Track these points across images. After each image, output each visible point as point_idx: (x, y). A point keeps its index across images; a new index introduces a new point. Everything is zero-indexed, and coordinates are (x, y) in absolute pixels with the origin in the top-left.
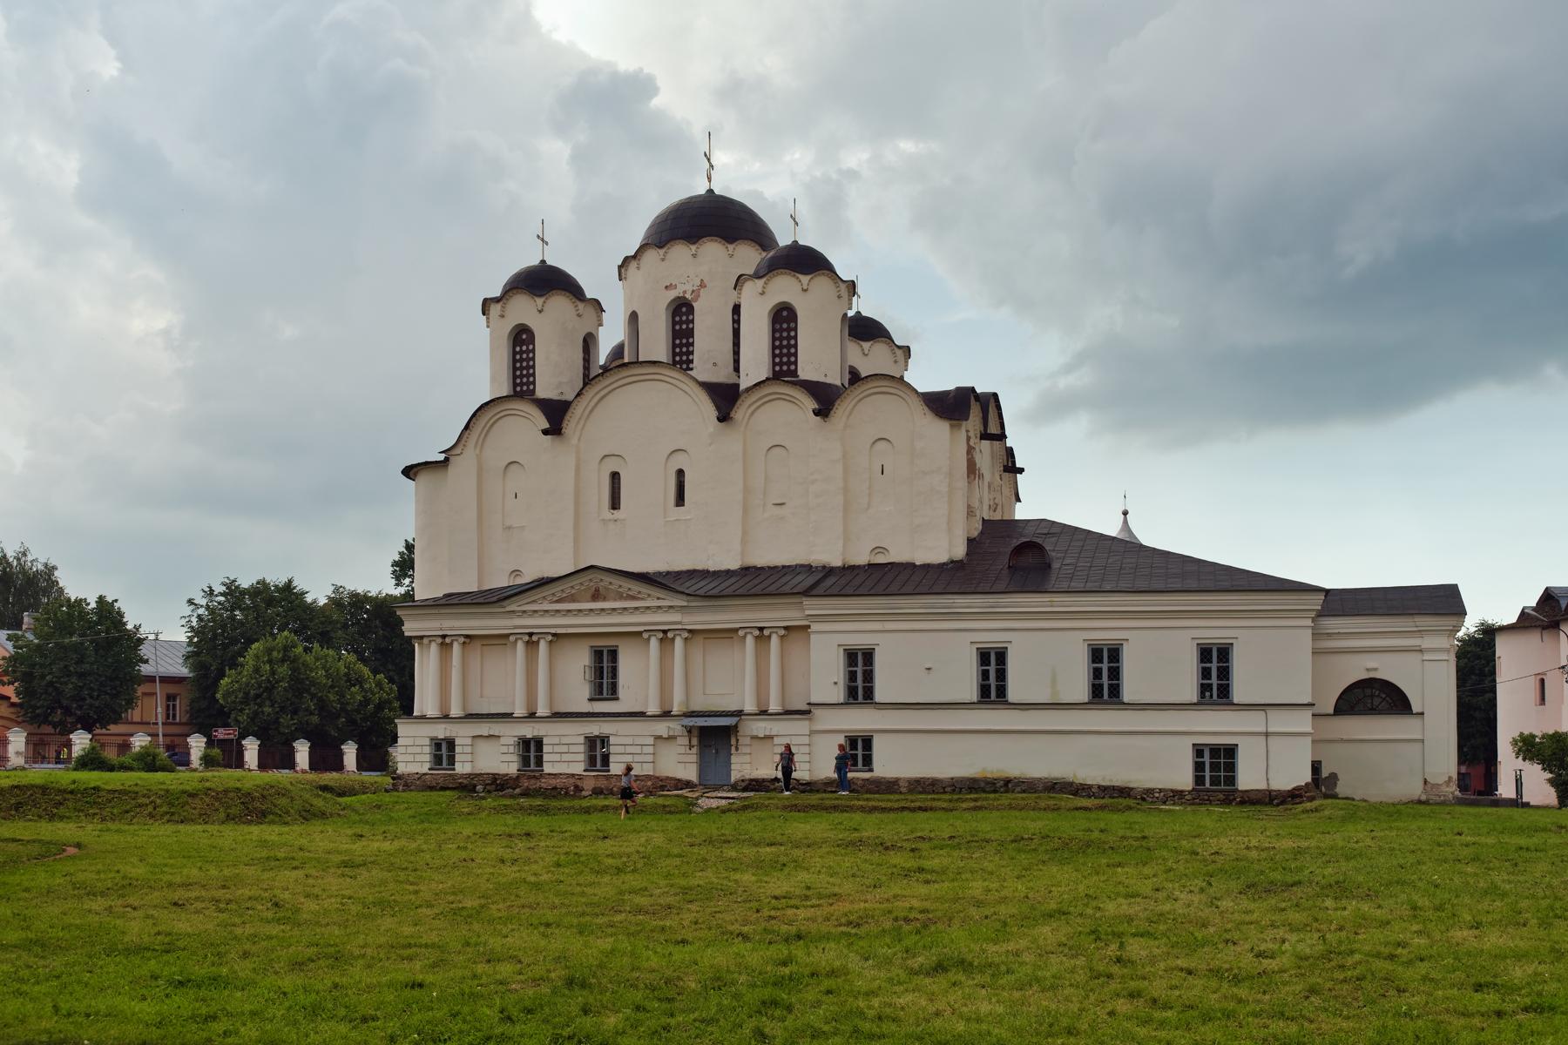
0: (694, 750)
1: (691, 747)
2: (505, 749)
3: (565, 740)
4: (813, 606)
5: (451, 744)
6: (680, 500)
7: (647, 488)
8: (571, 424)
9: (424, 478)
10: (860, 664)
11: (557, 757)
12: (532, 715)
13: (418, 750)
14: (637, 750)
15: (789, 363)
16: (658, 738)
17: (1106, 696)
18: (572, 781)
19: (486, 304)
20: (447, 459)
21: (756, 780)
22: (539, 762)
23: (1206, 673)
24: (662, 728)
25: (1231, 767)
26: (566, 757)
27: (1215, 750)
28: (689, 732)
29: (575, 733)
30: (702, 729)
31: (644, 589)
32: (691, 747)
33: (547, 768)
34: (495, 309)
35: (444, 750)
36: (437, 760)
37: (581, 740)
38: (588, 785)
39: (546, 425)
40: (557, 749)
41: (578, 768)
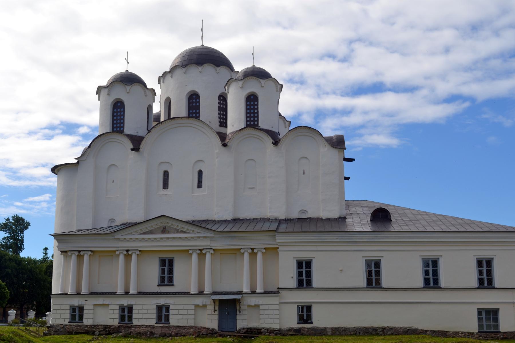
0: (217, 313)
1: (215, 311)
2: (112, 312)
3: (145, 307)
4: (280, 238)
5: (81, 309)
6: (200, 186)
7: (182, 179)
8: (143, 146)
9: (62, 173)
11: (141, 316)
12: (127, 293)
13: (63, 312)
14: (185, 312)
15: (254, 121)
16: (197, 306)
17: (432, 284)
18: (149, 329)
19: (100, 90)
20: (78, 162)
21: (251, 329)
22: (130, 318)
23: (480, 273)
24: (199, 301)
25: (496, 320)
26: (145, 316)
27: (488, 312)
28: (214, 303)
29: (152, 303)
30: (220, 301)
31: (191, 228)
32: (215, 311)
33: (135, 322)
34: (104, 92)
35: (77, 313)
36: (73, 317)
37: (155, 307)
38: (158, 331)
39: (132, 147)
40: (141, 311)
41: (153, 322)
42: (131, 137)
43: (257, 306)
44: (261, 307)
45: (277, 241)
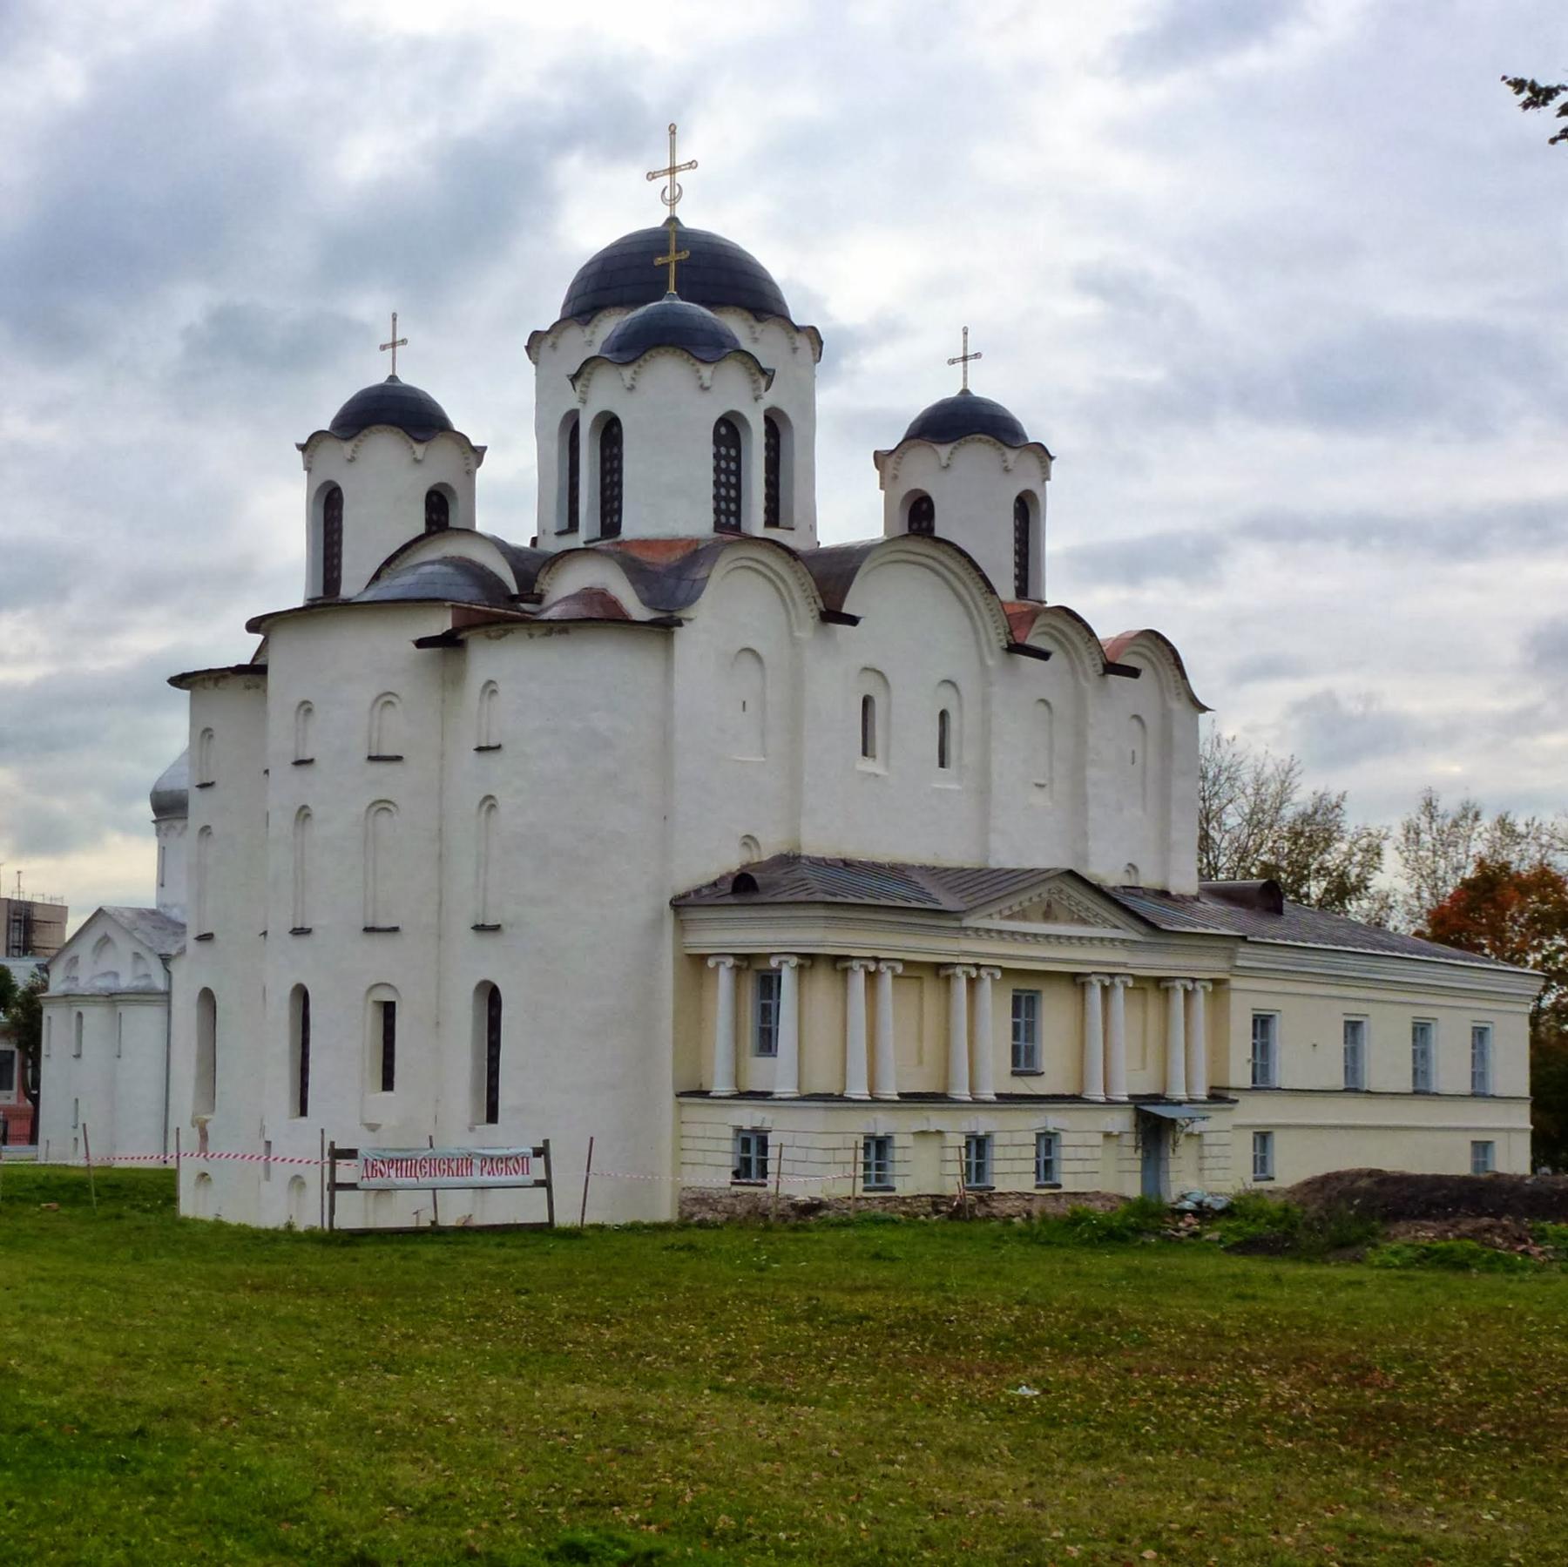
0: (1139, 1154)
1: (1137, 1148)
16: (1107, 1135)
43: (1200, 1135)
44: (1208, 1139)
45: (1239, 963)
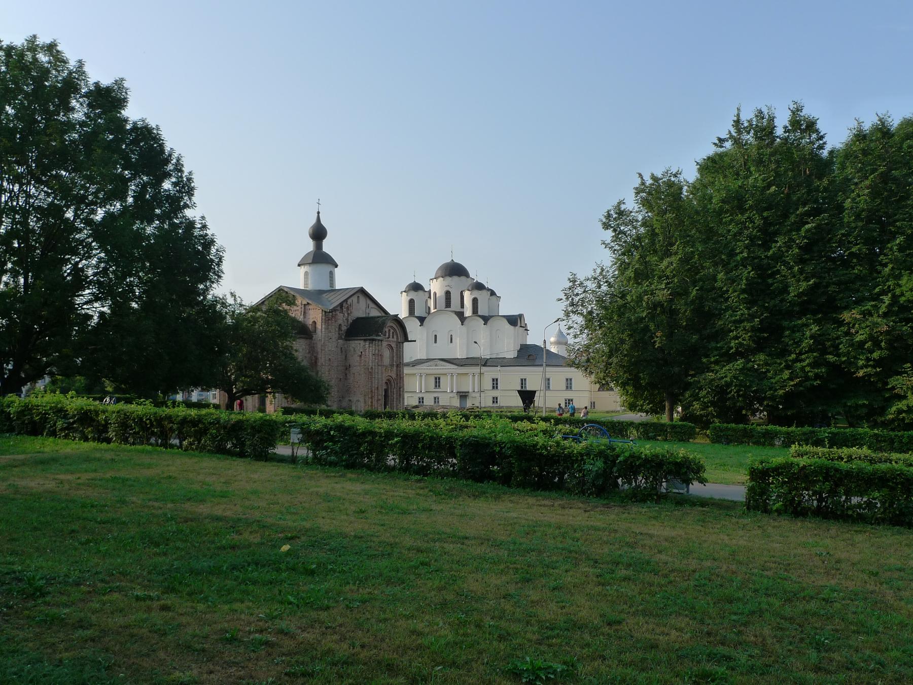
7: (443, 339)
10: (495, 383)
24: (451, 395)
41: (432, 403)
42: (417, 317)
